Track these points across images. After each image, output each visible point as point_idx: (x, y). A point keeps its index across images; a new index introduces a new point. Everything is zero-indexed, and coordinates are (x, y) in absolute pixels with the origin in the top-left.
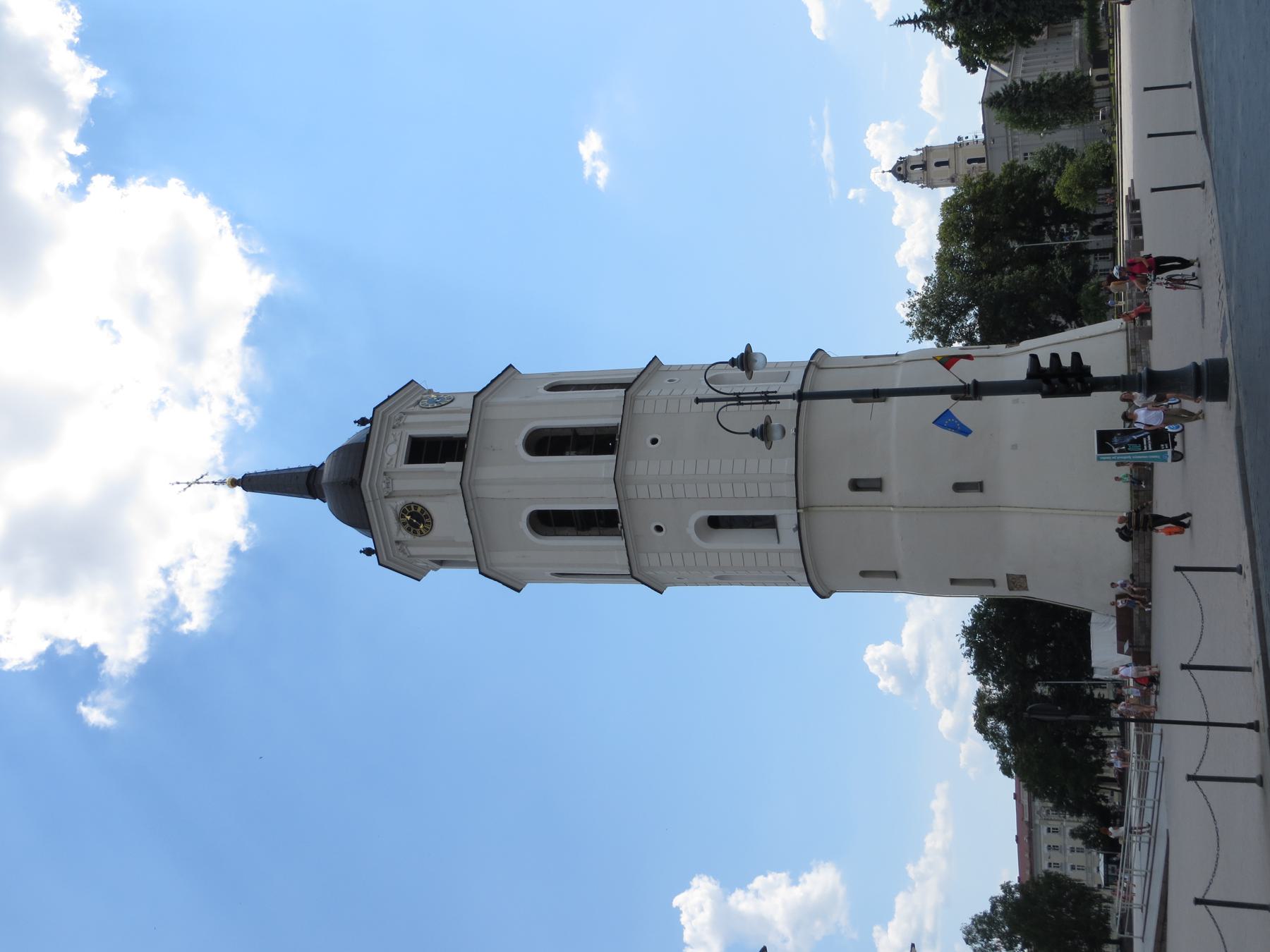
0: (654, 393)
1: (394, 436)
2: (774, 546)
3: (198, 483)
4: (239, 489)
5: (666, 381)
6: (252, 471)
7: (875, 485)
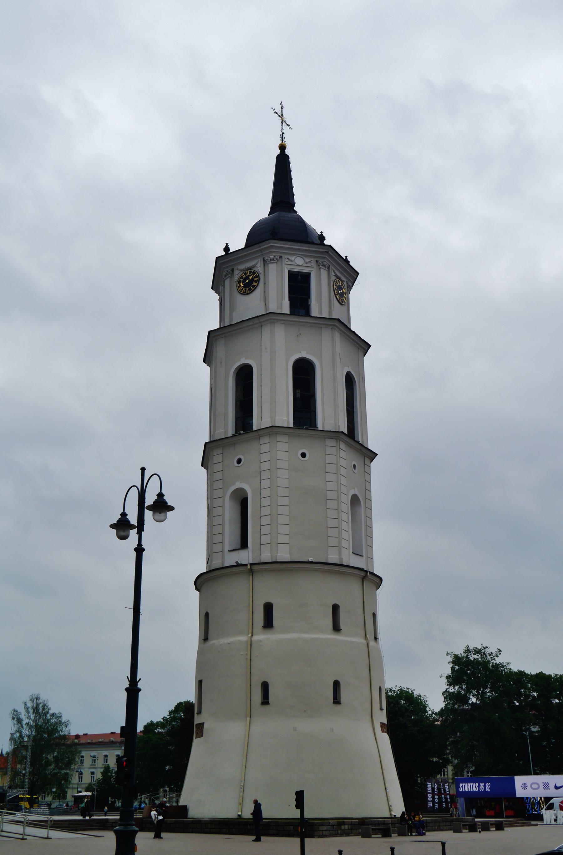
0: (343, 454)
1: (310, 262)
2: (227, 548)
3: (282, 123)
4: (278, 152)
5: (354, 463)
6: (291, 161)
7: (268, 623)
